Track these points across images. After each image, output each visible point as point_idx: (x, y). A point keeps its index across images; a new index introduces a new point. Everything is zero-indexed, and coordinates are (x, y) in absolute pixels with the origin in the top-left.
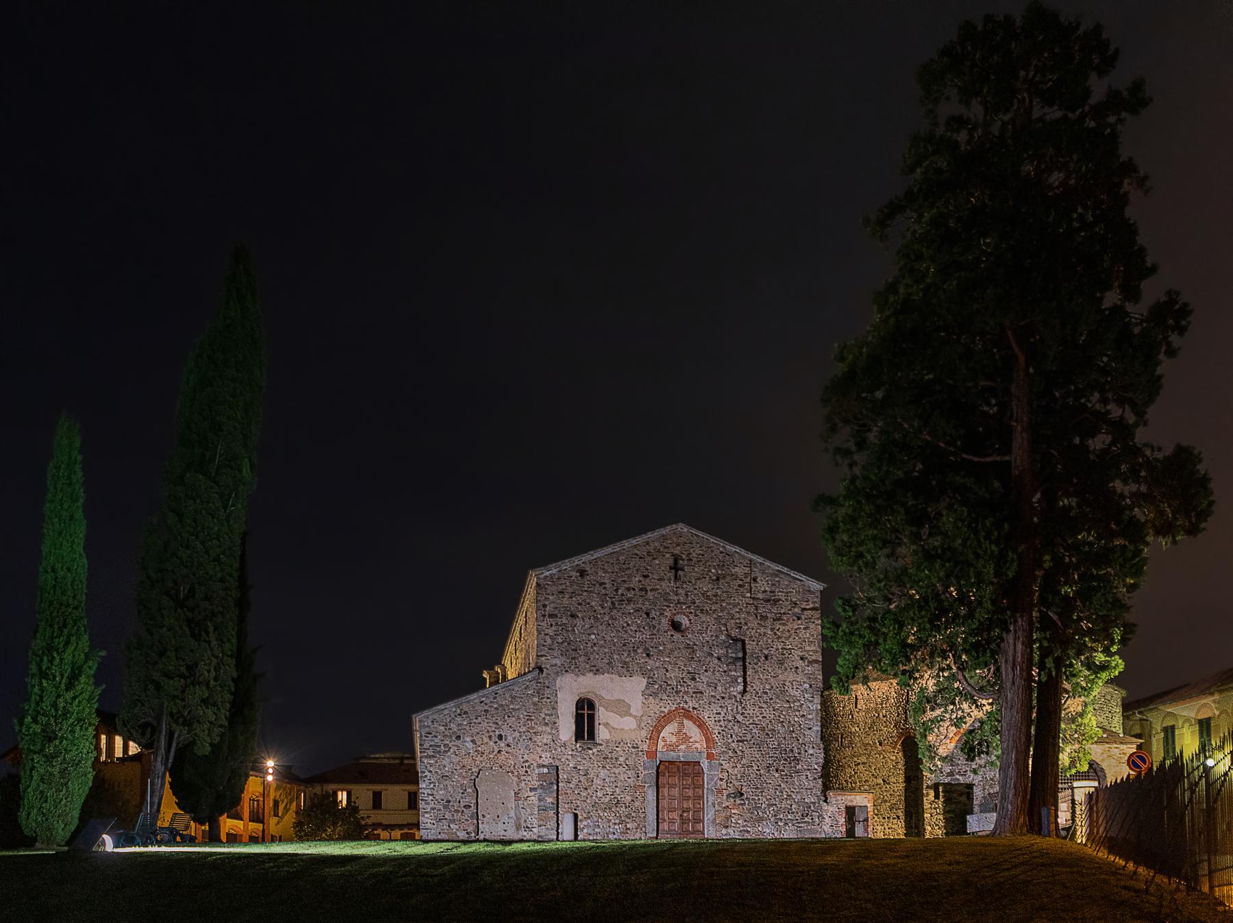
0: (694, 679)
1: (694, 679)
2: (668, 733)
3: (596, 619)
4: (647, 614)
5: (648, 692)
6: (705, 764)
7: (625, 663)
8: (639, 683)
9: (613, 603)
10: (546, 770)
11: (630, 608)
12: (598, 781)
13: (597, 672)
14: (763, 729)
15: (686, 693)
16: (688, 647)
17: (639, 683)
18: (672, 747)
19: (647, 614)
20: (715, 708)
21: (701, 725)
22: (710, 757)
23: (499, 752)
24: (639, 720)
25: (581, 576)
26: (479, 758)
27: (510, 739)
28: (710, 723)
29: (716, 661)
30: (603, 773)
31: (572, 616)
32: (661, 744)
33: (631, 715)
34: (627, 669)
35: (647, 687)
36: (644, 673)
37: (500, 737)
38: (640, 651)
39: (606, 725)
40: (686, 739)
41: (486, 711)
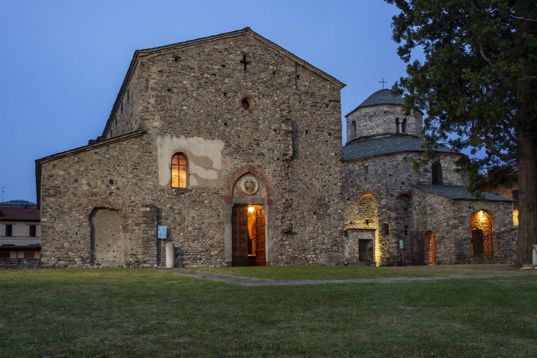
1: (258, 145)
3: (188, 94)
4: (225, 94)
5: (225, 152)
9: (200, 84)
10: (148, 209)
13: (188, 135)
14: (305, 184)
19: (225, 94)
23: (111, 194)
24: (220, 172)
25: (176, 60)
28: (270, 177)
29: (273, 133)
30: (193, 213)
31: (169, 90)
33: (213, 169)
34: (210, 135)
35: (224, 149)
36: (222, 137)
37: (111, 182)
38: (220, 121)
39: (196, 176)
41: (99, 160)
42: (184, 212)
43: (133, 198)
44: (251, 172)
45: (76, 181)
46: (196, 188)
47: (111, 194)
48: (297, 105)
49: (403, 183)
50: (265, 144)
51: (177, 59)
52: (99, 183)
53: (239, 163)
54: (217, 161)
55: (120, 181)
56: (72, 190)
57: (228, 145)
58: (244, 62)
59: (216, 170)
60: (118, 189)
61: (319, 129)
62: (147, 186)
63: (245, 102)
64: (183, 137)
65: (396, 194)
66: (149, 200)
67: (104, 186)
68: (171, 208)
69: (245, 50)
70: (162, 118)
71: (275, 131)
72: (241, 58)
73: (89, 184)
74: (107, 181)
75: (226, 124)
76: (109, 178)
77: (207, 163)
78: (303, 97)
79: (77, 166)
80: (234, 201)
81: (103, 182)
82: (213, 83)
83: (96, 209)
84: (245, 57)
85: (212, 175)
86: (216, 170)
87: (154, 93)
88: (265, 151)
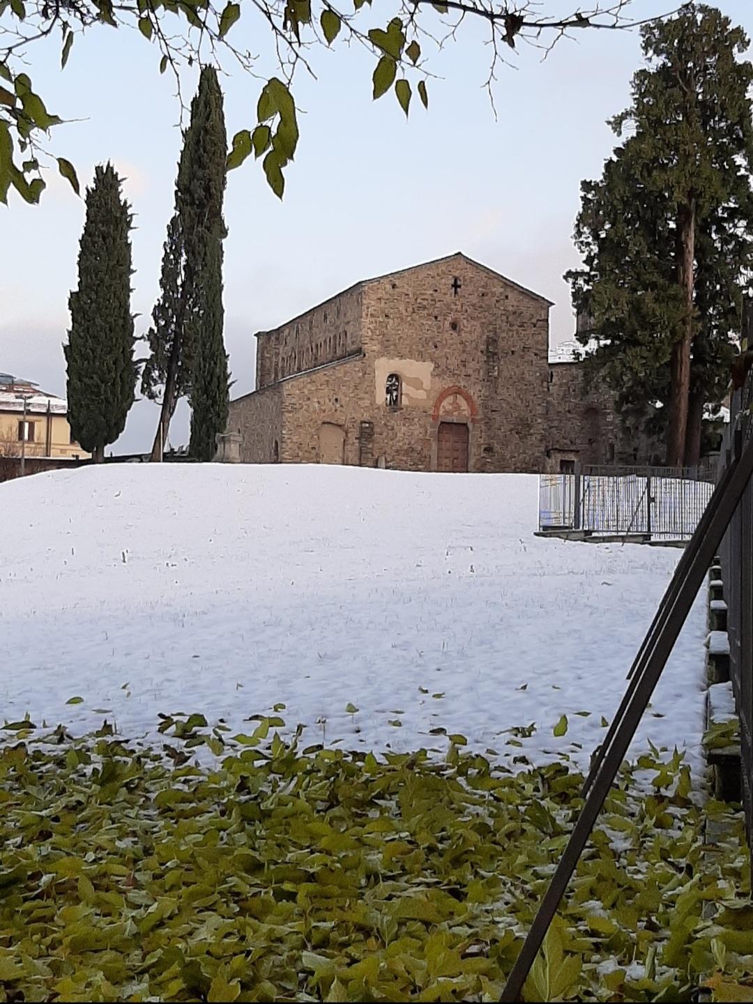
0: (464, 366)
1: (464, 366)
2: (447, 403)
7: (421, 352)
8: (429, 366)
13: (402, 357)
15: (460, 375)
16: (462, 343)
17: (429, 366)
21: (468, 399)
26: (322, 414)
27: (343, 403)
29: (480, 354)
32: (442, 410)
33: (423, 389)
34: (421, 357)
37: (336, 400)
39: (407, 395)
41: (328, 381)
43: (354, 415)
44: (458, 391)
45: (309, 399)
46: (407, 407)
47: (336, 410)
52: (327, 401)
53: (448, 383)
54: (427, 382)
55: (344, 400)
56: (305, 407)
59: (426, 390)
60: (342, 406)
62: (366, 405)
64: (397, 359)
66: (366, 417)
67: (331, 403)
68: (385, 424)
70: (381, 343)
71: (482, 352)
73: (319, 402)
74: (333, 400)
75: (436, 347)
76: (335, 397)
77: (417, 384)
79: (309, 386)
81: (330, 400)
83: (324, 423)
85: (421, 395)
86: (426, 390)
87: (373, 319)
88: (470, 372)
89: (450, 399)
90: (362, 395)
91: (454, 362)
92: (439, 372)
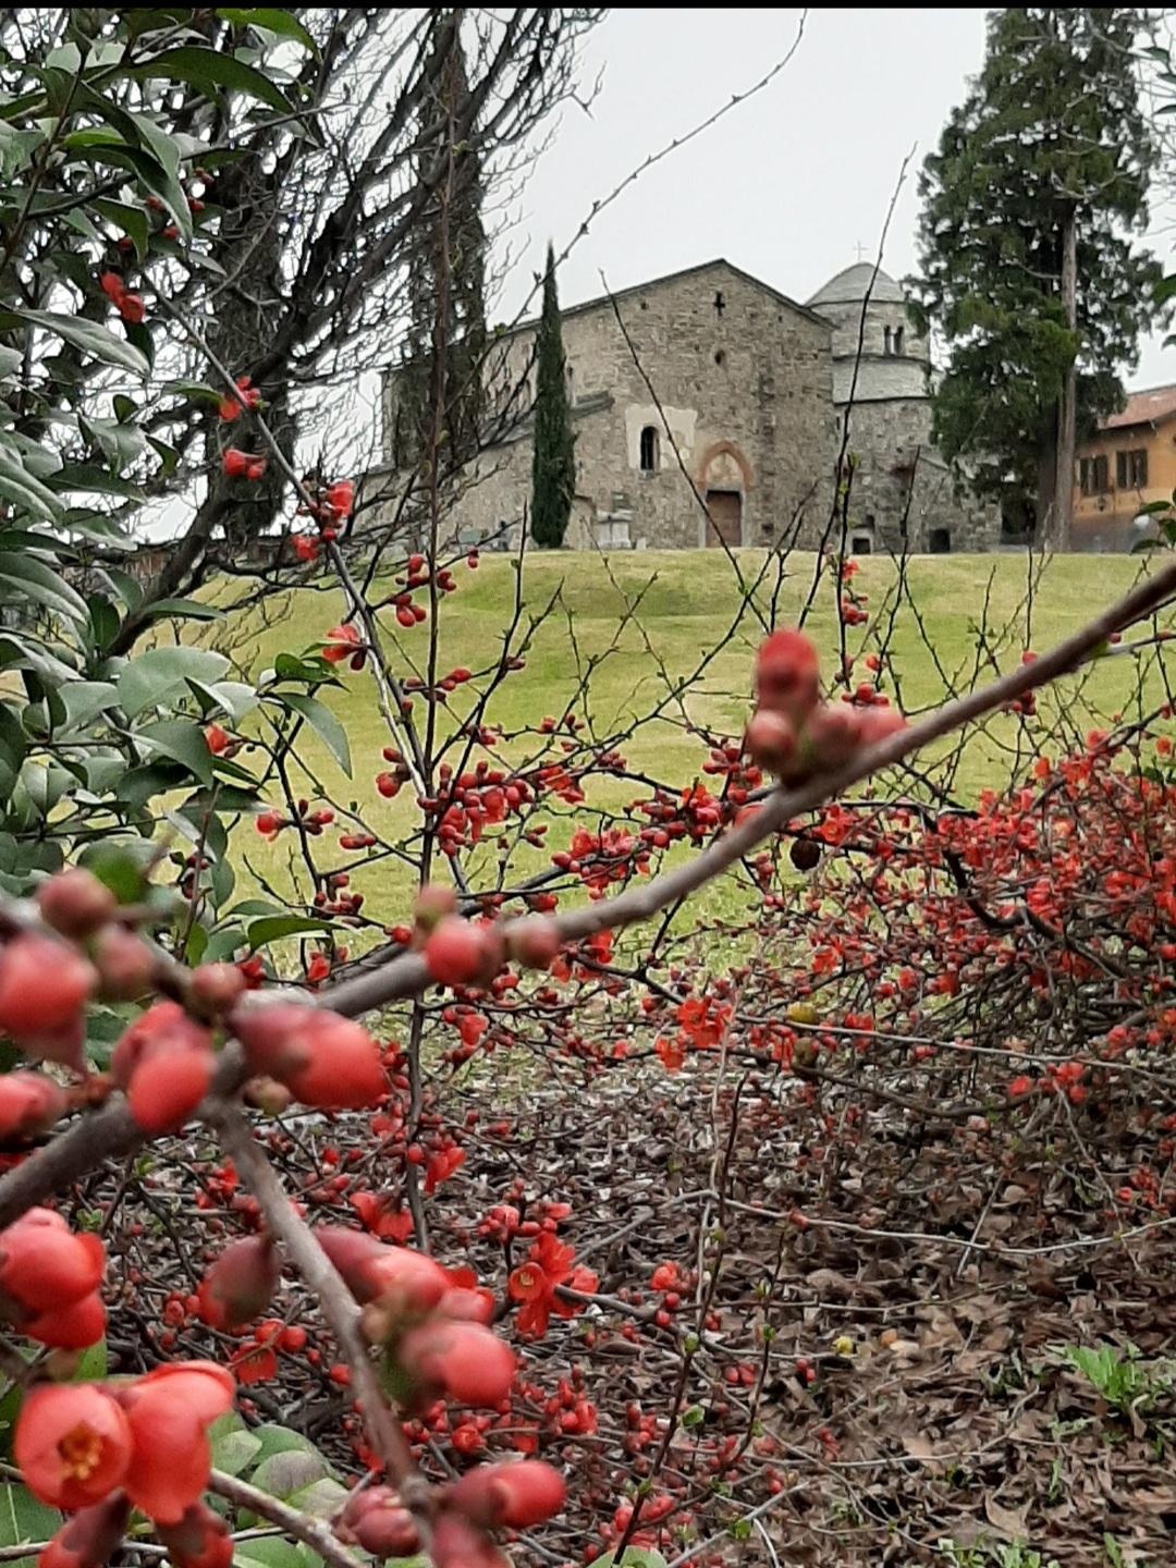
2: (715, 465)
4: (697, 348)
6: (744, 494)
8: (693, 414)
11: (683, 342)
12: (660, 510)
16: (729, 382)
18: (716, 478)
19: (697, 348)
20: (750, 442)
21: (739, 458)
22: (749, 489)
28: (748, 456)
34: (682, 402)
36: (696, 406)
40: (728, 471)
42: (655, 501)
44: (726, 449)
46: (667, 470)
48: (781, 359)
49: (899, 450)
50: (744, 412)
51: (644, 306)
53: (713, 438)
57: (701, 416)
58: (719, 304)
61: (806, 389)
63: (719, 358)
65: (888, 469)
66: (619, 487)
69: (719, 289)
70: (631, 385)
72: (714, 299)
75: (699, 388)
78: (786, 349)
80: (708, 487)
82: (682, 335)
84: (719, 295)
88: (741, 422)
89: (718, 459)
90: (612, 457)
91: (721, 409)
92: (706, 421)
